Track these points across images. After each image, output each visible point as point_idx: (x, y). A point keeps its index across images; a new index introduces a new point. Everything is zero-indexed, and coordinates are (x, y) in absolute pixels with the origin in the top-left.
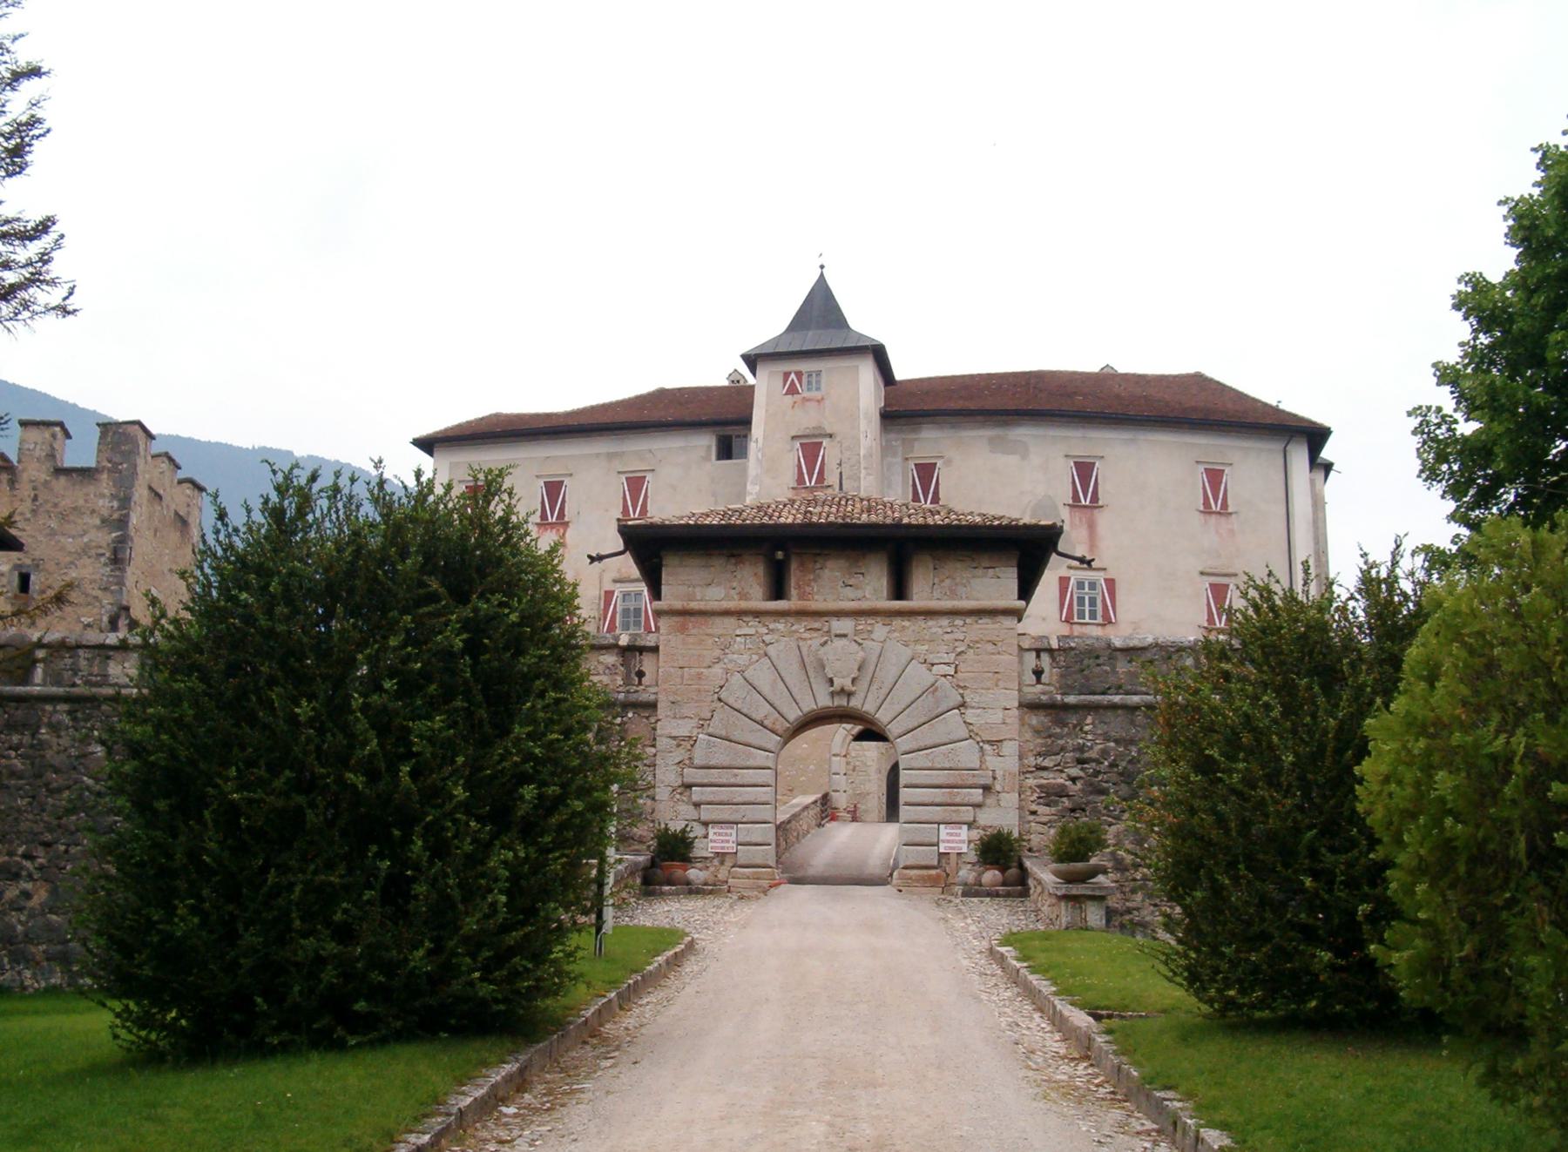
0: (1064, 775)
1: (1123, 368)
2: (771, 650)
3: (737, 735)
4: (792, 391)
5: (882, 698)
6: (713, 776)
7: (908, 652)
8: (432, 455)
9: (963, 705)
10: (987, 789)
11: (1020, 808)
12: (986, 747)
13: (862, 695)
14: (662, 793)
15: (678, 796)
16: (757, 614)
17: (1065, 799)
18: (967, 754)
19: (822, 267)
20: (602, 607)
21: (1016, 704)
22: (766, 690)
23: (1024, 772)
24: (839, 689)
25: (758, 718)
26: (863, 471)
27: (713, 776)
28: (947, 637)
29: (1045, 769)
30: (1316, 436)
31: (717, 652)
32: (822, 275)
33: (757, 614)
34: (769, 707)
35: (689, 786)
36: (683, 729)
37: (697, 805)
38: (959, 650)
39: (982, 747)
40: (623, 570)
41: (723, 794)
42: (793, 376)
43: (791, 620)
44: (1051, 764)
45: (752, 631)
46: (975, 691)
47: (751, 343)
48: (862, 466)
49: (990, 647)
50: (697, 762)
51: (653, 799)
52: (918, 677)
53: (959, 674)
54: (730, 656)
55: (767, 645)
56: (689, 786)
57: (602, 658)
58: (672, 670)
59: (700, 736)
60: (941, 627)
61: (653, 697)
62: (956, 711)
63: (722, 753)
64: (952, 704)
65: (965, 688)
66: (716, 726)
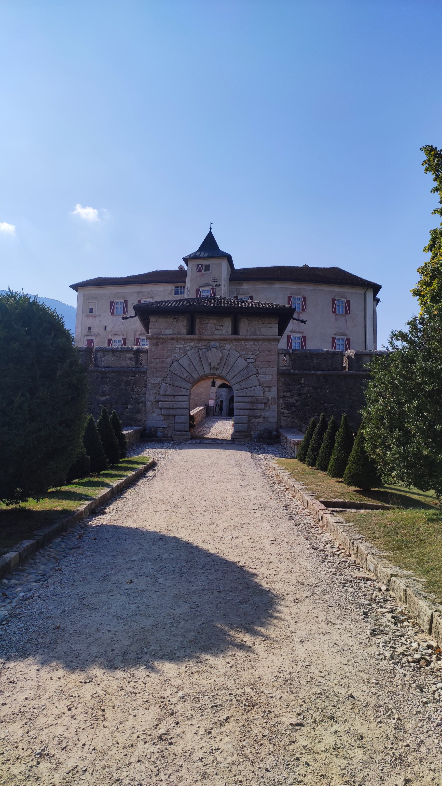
0: (293, 399)
1: (310, 265)
2: (189, 353)
5: (228, 370)
6: (167, 398)
7: (237, 354)
8: (77, 291)
9: (257, 374)
10: (265, 403)
11: (278, 411)
12: (265, 388)
13: (221, 369)
14: (149, 404)
15: (154, 405)
16: (184, 340)
17: (293, 408)
18: (259, 392)
19: (211, 228)
21: (277, 373)
22: (187, 368)
23: (278, 398)
24: (213, 367)
25: (183, 377)
27: (167, 398)
28: (252, 349)
29: (287, 397)
30: (376, 288)
31: (169, 353)
32: (210, 231)
33: (184, 340)
34: (187, 373)
35: (158, 402)
36: (157, 381)
37: (161, 409)
38: (256, 353)
39: (264, 389)
41: (171, 405)
42: (200, 266)
43: (196, 341)
44: (289, 395)
45: (182, 346)
46: (262, 368)
47: (186, 254)
49: (267, 352)
50: (161, 393)
51: (145, 406)
52: (242, 363)
53: (256, 362)
54: (174, 355)
55: (187, 351)
56: (158, 402)
57: (127, 355)
58: (153, 360)
59: (163, 384)
60: (250, 345)
61: (145, 369)
62: (255, 375)
63: (170, 391)
64: (254, 373)
65: (258, 367)
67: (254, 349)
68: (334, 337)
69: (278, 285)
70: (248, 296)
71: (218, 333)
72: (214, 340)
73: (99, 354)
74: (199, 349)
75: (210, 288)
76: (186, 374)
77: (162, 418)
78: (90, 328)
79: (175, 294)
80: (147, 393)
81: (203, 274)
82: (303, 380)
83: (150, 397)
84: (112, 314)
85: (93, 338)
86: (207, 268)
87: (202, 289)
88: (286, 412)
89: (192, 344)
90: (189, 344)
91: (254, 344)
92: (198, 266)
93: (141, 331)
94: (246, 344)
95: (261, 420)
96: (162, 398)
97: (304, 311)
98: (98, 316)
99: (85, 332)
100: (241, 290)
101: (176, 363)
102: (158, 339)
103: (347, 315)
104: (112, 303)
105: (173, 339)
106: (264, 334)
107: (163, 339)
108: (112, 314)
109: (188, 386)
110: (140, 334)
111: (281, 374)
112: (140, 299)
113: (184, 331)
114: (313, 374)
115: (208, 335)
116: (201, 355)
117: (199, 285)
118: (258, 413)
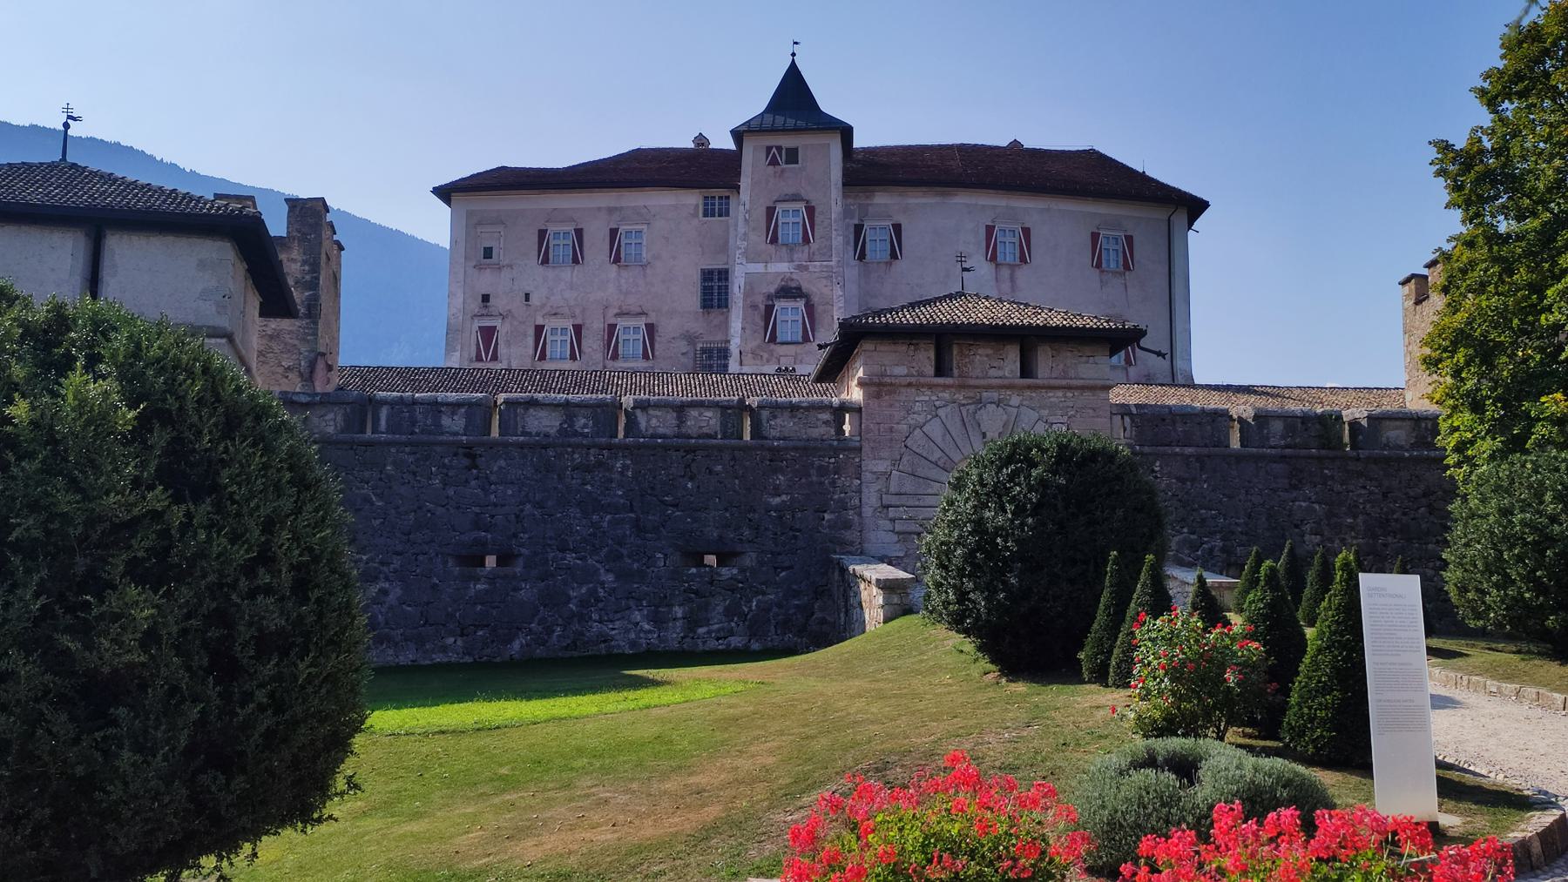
1: (1028, 143)
2: (941, 412)
3: (920, 472)
4: (774, 162)
14: (867, 512)
16: (930, 387)
19: (793, 55)
20: (606, 337)
22: (939, 440)
25: (933, 460)
26: (834, 232)
32: (793, 60)
35: (888, 507)
36: (882, 466)
37: (893, 520)
38: (1069, 414)
40: (624, 307)
42: (774, 149)
43: (953, 390)
45: (927, 398)
48: (833, 228)
49: (1091, 411)
55: (937, 408)
56: (888, 507)
61: (858, 444)
63: (909, 486)
67: (1065, 404)
69: (963, 199)
70: (890, 223)
72: (988, 388)
73: (765, 414)
75: (801, 206)
76: (937, 454)
77: (896, 538)
78: (486, 298)
79: (705, 215)
80: (865, 490)
81: (783, 171)
82: (1158, 464)
83: (871, 498)
84: (542, 264)
85: (497, 323)
86: (792, 156)
87: (780, 208)
89: (946, 395)
90: (940, 395)
92: (769, 149)
93: (620, 308)
94: (1051, 394)
96: (894, 500)
97: (1026, 262)
98: (508, 266)
99: (475, 306)
100: (870, 208)
102: (880, 384)
104: (542, 234)
105: (910, 385)
106: (1084, 376)
107: (891, 384)
110: (617, 315)
112: (615, 226)
113: (930, 370)
114: (1176, 454)
115: (977, 378)
116: (965, 417)
117: (775, 198)
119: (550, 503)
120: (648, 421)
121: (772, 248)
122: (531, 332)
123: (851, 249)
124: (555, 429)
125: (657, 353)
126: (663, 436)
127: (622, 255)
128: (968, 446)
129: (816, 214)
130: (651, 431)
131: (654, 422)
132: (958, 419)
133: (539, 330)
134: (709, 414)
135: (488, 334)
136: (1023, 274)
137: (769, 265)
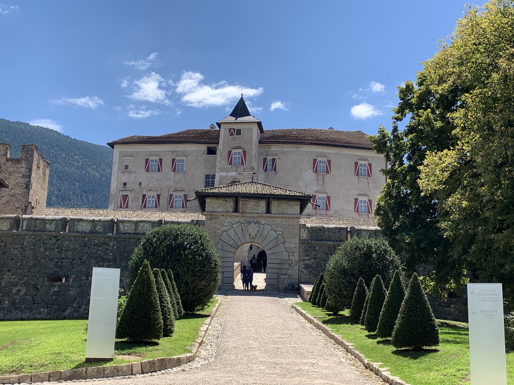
2: (234, 226)
9: (284, 243)
11: (299, 270)
18: (285, 256)
26: (253, 161)
29: (306, 260)
31: (219, 226)
42: (232, 130)
46: (287, 238)
52: (273, 234)
64: (281, 242)
65: (285, 237)
66: (219, 246)
68: (356, 197)
71: (256, 212)
74: (242, 223)
76: (232, 242)
78: (125, 184)
81: (235, 138)
82: (318, 247)
84: (146, 171)
87: (234, 151)
88: (305, 271)
90: (235, 219)
91: (282, 221)
92: (230, 129)
95: (286, 276)
97: (329, 173)
98: (134, 172)
99: (121, 187)
100: (269, 152)
101: (225, 232)
103: (369, 178)
104: (147, 160)
108: (146, 171)
109: (233, 250)
111: (302, 242)
118: (285, 272)
119: (84, 258)
120: (124, 227)
121: (230, 166)
122: (141, 197)
123: (262, 167)
124: (89, 230)
125: (187, 206)
126: (129, 234)
127: (176, 169)
128: (244, 239)
129: (247, 154)
130: (125, 231)
131: (126, 228)
132: (240, 228)
133: (144, 196)
134: (147, 225)
135: (125, 197)
136: (328, 177)
137: (228, 173)
